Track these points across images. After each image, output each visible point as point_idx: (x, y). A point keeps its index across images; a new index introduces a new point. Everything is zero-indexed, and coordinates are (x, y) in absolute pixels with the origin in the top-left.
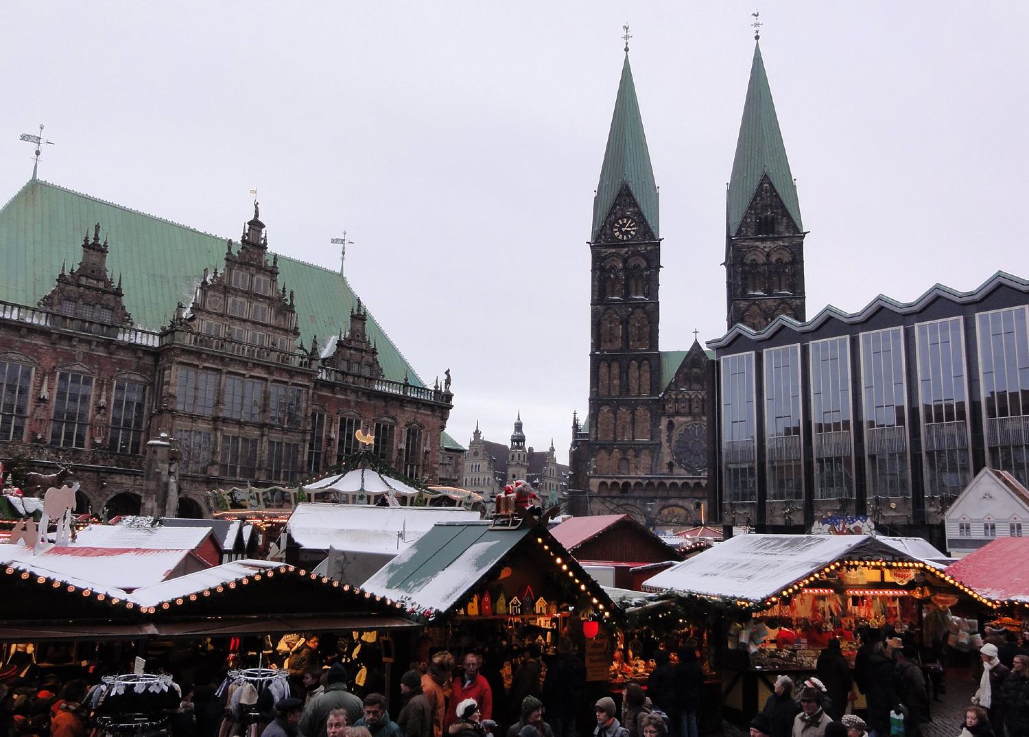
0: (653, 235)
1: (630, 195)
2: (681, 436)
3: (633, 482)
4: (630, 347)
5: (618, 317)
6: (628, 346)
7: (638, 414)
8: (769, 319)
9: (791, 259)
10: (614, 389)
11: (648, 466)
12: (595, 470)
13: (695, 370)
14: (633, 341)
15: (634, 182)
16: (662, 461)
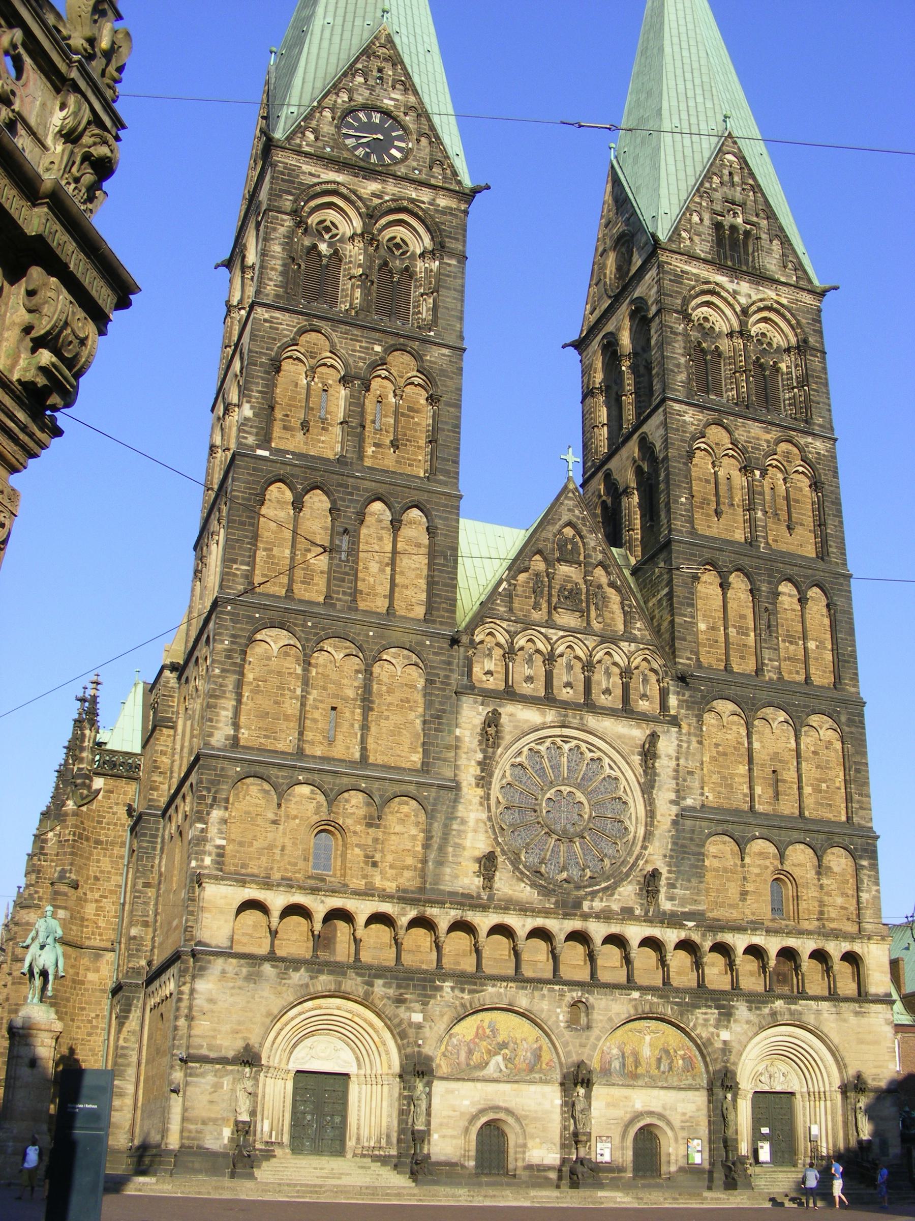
0: (455, 174)
1: (396, 60)
2: (518, 771)
3: (362, 909)
4: (368, 463)
5: (339, 365)
6: (361, 456)
7: (384, 677)
8: (757, 473)
9: (793, 340)
10: (307, 581)
11: (409, 861)
12: (221, 853)
14: (375, 445)
15: (405, 39)
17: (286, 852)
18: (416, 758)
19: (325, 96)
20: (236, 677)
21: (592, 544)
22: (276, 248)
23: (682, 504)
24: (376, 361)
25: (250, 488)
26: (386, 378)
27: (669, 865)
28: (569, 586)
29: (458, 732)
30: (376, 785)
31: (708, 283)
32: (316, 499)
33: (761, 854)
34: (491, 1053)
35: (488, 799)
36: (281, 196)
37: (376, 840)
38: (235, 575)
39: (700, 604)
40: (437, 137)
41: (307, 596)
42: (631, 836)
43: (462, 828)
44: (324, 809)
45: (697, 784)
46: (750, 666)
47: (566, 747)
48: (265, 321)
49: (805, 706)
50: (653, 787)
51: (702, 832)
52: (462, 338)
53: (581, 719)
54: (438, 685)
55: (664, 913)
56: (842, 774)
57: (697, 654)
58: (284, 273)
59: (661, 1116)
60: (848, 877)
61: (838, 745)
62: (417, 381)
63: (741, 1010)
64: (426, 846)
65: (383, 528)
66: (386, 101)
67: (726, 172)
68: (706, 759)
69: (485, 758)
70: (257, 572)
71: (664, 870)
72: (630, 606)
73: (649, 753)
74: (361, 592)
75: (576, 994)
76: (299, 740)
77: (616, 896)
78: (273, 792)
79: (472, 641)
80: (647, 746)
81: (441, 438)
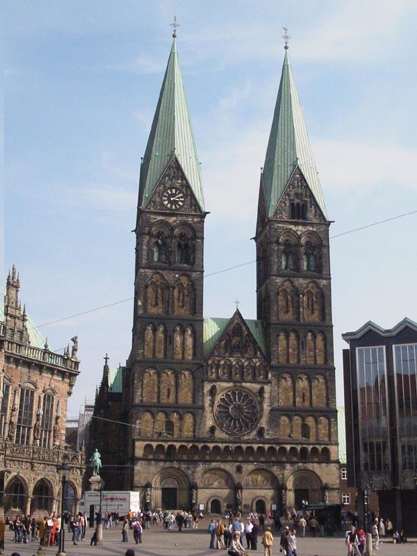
0: (199, 208)
1: (179, 168)
3: (177, 445)
4: (176, 313)
6: (173, 311)
10: (159, 352)
13: (236, 338)
16: (205, 424)
34: (215, 481)
39: (280, 343)
46: (295, 361)
52: (203, 267)
58: (148, 256)
59: (263, 497)
63: (288, 466)
67: (296, 182)
73: (261, 391)
75: (238, 464)
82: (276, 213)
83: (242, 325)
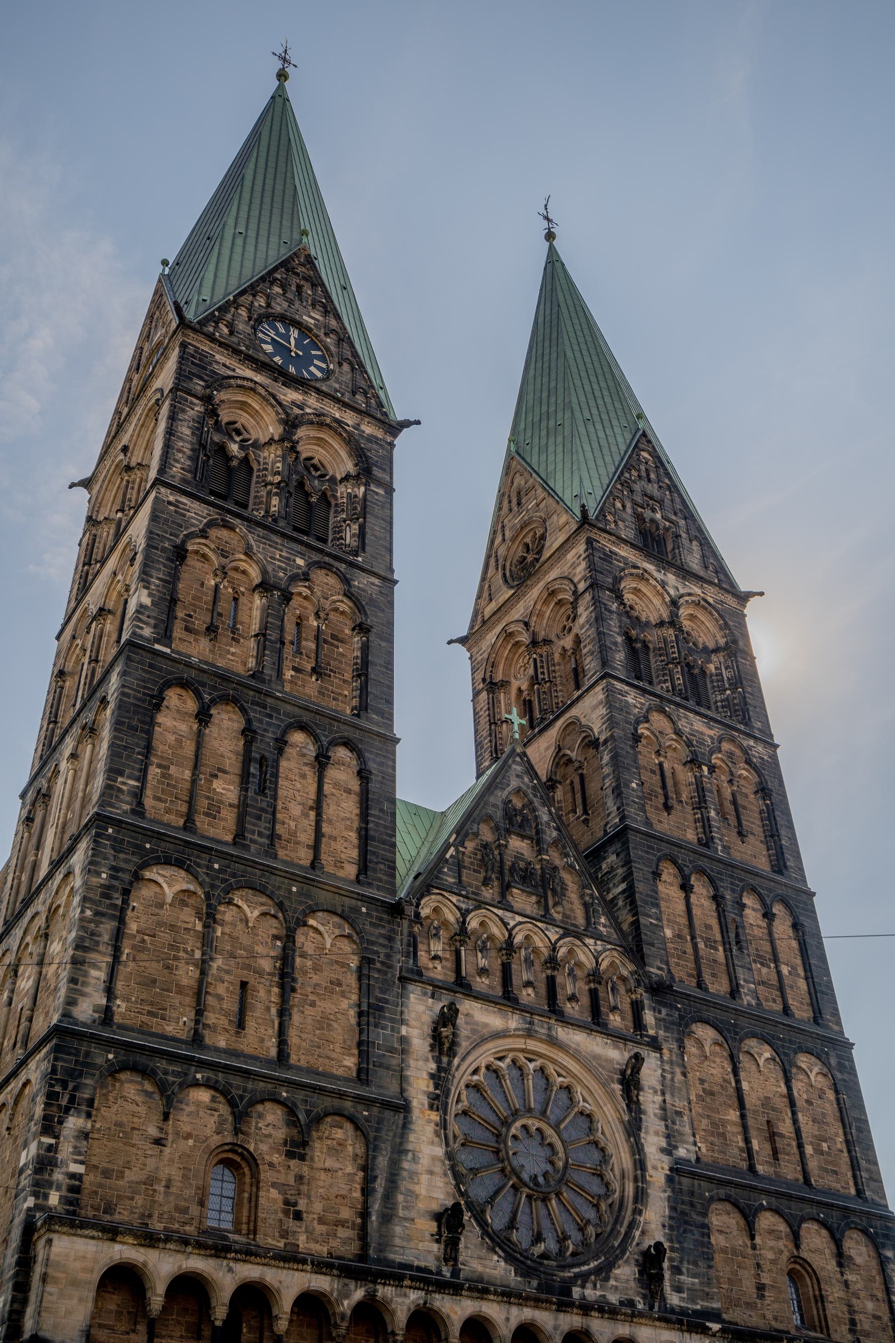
2: (474, 1095)
4: (287, 688)
7: (309, 948)
8: (705, 769)
9: (722, 642)
10: (213, 812)
11: (346, 1213)
12: (75, 1186)
14: (295, 669)
17: (173, 1190)
18: (350, 1061)
19: (243, 293)
20: (115, 924)
21: (545, 818)
22: (185, 430)
23: (633, 790)
24: (297, 575)
25: (145, 688)
26: (306, 598)
27: (671, 1240)
28: (522, 865)
29: (404, 1030)
30: (300, 1095)
31: (638, 568)
32: (224, 716)
33: (771, 1232)
35: (445, 1129)
36: (191, 379)
37: (300, 1178)
38: (120, 790)
40: (361, 365)
41: (212, 832)
42: (617, 1195)
43: (414, 1167)
44: (229, 1126)
45: (687, 1130)
47: (531, 1066)
48: (169, 503)
49: (791, 1042)
50: (639, 1129)
51: (702, 1196)
52: (392, 571)
53: (549, 1029)
54: (378, 965)
55: (672, 1311)
56: (841, 1132)
57: (667, 964)
58: (194, 458)
60: (874, 1272)
61: (831, 1095)
62: (342, 607)
64: (367, 1191)
65: (306, 764)
66: (305, 317)
67: (643, 468)
68: (693, 1098)
69: (439, 1069)
70: (149, 792)
71: (666, 1245)
72: (592, 896)
74: (279, 837)
76: (197, 1022)
77: (612, 1282)
78: (157, 1096)
79: (417, 915)
80: (629, 1072)
81: (373, 673)
82: (602, 513)
83: (537, 802)
